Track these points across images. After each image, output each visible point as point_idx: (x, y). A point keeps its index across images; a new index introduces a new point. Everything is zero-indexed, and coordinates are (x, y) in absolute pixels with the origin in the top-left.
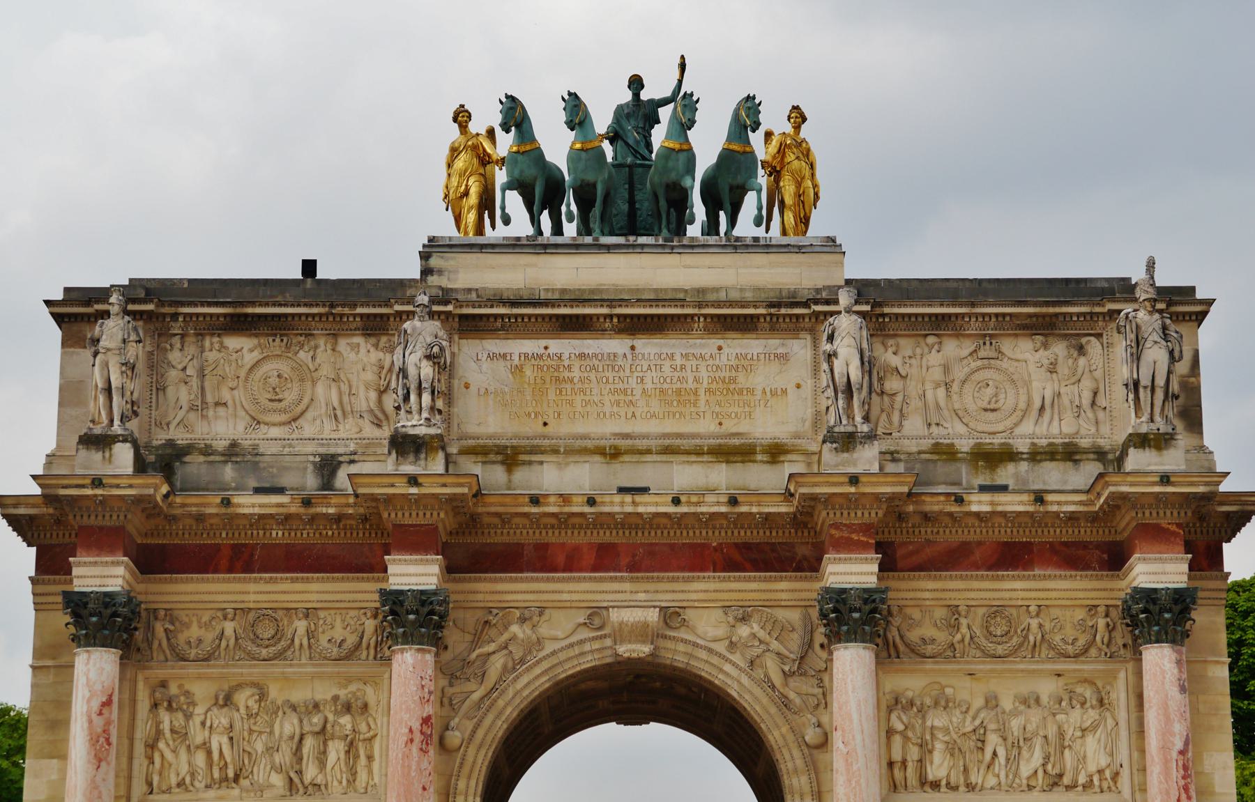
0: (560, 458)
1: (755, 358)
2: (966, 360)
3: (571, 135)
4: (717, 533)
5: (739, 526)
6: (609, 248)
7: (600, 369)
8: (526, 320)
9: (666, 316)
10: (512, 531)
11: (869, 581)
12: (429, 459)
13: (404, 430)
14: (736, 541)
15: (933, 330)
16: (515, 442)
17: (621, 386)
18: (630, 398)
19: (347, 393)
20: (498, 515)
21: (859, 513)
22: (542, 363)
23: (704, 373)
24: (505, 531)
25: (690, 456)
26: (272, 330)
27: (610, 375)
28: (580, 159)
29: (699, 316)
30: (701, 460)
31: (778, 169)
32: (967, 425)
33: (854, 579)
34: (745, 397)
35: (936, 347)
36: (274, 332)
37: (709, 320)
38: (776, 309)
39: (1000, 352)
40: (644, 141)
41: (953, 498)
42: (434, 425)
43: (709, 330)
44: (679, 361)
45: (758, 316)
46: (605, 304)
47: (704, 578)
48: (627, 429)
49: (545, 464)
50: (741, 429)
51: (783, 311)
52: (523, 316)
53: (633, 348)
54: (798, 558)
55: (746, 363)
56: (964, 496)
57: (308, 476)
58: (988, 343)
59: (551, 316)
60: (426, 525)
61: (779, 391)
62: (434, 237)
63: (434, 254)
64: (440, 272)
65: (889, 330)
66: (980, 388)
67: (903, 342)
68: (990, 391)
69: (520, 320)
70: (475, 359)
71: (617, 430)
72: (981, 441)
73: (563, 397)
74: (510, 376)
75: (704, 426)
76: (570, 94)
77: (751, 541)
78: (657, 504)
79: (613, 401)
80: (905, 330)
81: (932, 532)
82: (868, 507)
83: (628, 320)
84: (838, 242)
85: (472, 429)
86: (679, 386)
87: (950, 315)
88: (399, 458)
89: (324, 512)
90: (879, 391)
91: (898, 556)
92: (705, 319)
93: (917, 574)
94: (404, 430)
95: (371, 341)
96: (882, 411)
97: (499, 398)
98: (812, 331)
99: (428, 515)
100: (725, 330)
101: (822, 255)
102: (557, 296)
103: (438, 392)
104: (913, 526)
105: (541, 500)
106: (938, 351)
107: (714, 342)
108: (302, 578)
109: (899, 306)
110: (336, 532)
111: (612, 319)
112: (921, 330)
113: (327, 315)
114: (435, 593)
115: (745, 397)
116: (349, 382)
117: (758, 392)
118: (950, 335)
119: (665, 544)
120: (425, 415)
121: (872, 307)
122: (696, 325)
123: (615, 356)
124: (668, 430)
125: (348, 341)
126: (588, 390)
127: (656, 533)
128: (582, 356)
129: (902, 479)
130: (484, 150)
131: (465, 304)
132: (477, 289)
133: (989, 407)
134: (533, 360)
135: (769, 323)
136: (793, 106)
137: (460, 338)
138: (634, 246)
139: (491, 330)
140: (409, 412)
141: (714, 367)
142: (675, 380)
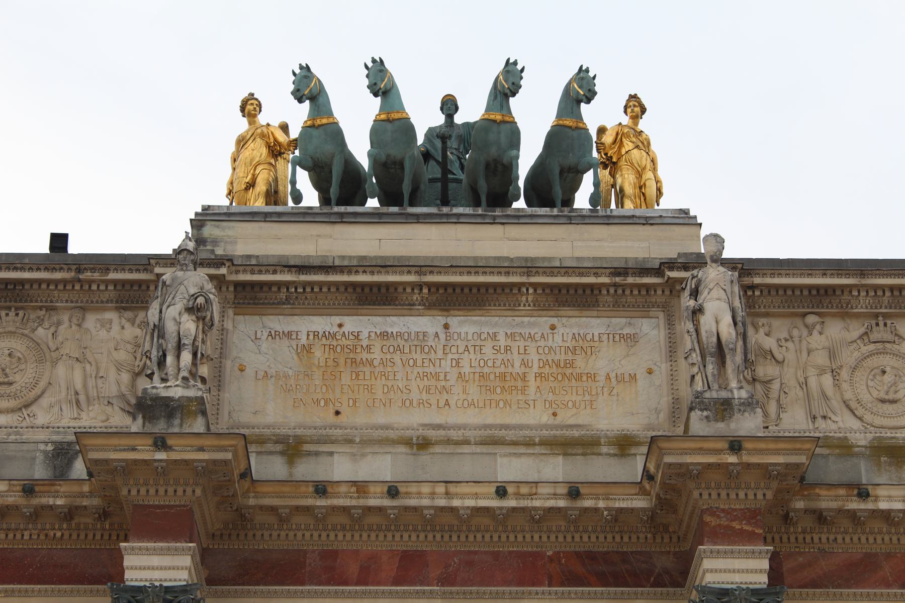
0: (354, 449)
1: (596, 338)
2: (855, 345)
3: (376, 102)
4: (553, 538)
5: (581, 529)
6: (418, 219)
7: (407, 350)
8: (316, 289)
9: (487, 286)
10: (291, 534)
11: (758, 581)
12: (184, 425)
13: (154, 391)
14: (577, 549)
15: (813, 307)
16: (299, 432)
17: (431, 369)
18: (443, 383)
19: (94, 376)
20: (273, 509)
21: (742, 495)
22: (335, 343)
23: (534, 357)
24: (283, 534)
25: (517, 447)
26: (5, 302)
27: (418, 356)
30: (532, 452)
31: (614, 160)
32: (860, 419)
33: (737, 578)
35: (818, 327)
36: (8, 304)
38: (622, 278)
39: (896, 335)
40: (458, 162)
41: (856, 492)
42: (194, 386)
43: (539, 306)
44: (502, 341)
46: (413, 269)
47: (537, 593)
48: (438, 420)
49: (336, 456)
50: (580, 422)
51: (630, 280)
52: (312, 284)
53: (446, 326)
54: (657, 571)
55: (586, 344)
56: (870, 488)
57: (37, 468)
58: (881, 323)
59: (347, 285)
60: (177, 506)
61: (627, 378)
62: (209, 206)
63: (208, 223)
64: (215, 242)
65: (759, 307)
66: (874, 376)
67: (776, 323)
69: (308, 289)
70: (253, 338)
71: (427, 421)
72: (881, 435)
73: (360, 382)
74: (295, 357)
76: (374, 61)
77: (596, 549)
78: (476, 496)
79: (421, 387)
80: (779, 307)
81: (828, 539)
82: (753, 485)
83: (441, 291)
84: (692, 214)
85: (245, 417)
86: (503, 369)
88: (147, 424)
89: (51, 503)
91: (784, 569)
92: (535, 290)
93: (811, 591)
94: (154, 391)
95: (126, 315)
97: (281, 383)
99: (180, 492)
100: (559, 306)
101: (674, 227)
102: (355, 263)
103: (202, 355)
104: (804, 532)
105: (329, 490)
107: (545, 321)
108: (20, 591)
109: (772, 275)
110: (67, 534)
111: (421, 289)
112: (799, 307)
113: (73, 281)
114: (184, 590)
115: (585, 384)
116: (97, 363)
117: (601, 378)
118: (834, 315)
119: (486, 553)
120: (185, 373)
122: (524, 298)
123: (424, 336)
124: (489, 421)
125: (99, 317)
126: (391, 374)
127: (475, 537)
128: (384, 335)
129: (798, 446)
130: (275, 140)
131: (241, 268)
132: (258, 256)
133: (887, 397)
134: (324, 339)
136: (630, 95)
137: (235, 314)
138: (447, 215)
139: (274, 304)
140: (164, 380)
141: (546, 350)
142: (498, 363)
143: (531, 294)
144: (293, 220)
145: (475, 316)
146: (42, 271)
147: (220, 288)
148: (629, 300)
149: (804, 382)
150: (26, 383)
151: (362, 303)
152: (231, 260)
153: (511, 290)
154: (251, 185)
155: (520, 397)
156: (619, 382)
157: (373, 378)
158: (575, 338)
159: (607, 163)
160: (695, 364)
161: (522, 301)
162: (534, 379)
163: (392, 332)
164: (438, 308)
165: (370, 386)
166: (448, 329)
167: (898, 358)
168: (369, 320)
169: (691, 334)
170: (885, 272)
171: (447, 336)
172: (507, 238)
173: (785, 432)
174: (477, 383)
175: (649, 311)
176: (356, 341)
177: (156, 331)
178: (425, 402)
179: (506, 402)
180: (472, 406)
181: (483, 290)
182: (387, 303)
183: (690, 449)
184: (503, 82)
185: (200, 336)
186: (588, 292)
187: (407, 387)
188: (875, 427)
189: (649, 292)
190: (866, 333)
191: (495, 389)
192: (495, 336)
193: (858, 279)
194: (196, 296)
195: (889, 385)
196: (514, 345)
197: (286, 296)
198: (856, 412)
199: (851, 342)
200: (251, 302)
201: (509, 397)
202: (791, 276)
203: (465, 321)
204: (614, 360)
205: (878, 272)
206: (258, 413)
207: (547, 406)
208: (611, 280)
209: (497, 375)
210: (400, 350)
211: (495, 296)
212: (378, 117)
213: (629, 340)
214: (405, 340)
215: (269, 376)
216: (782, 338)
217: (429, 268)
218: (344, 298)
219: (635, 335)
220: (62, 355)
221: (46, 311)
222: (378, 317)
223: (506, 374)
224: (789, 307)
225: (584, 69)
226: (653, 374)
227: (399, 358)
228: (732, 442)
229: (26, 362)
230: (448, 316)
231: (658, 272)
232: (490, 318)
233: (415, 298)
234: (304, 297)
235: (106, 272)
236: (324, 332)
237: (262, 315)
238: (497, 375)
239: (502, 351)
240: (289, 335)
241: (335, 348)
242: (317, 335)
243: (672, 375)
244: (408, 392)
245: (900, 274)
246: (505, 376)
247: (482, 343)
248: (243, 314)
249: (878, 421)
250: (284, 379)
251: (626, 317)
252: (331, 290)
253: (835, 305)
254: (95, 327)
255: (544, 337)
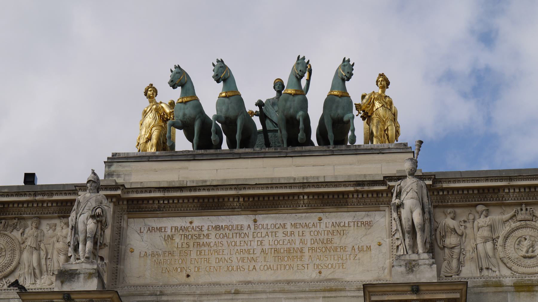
1: (347, 225)
2: (508, 223)
7: (231, 236)
15: (481, 201)
17: (245, 247)
18: (252, 256)
19: (44, 258)
27: (238, 240)
28: (224, 103)
29: (303, 194)
31: (369, 114)
32: (510, 269)
34: (339, 253)
35: (484, 213)
37: (311, 197)
39: (534, 216)
44: (289, 229)
45: (348, 193)
50: (336, 276)
51: (366, 188)
52: (173, 198)
53: (255, 221)
55: (341, 229)
58: (524, 209)
59: (194, 198)
61: (365, 249)
65: (448, 202)
66: (520, 242)
67: (458, 211)
68: (526, 243)
69: (171, 201)
70: (139, 232)
71: (242, 279)
73: (202, 257)
74: (164, 243)
75: (311, 274)
76: (218, 61)
79: (239, 259)
80: (460, 201)
83: (251, 200)
84: (409, 146)
86: (289, 246)
87: (494, 188)
90: (441, 246)
92: (308, 197)
95: (64, 221)
96: (445, 260)
98: (388, 203)
100: (324, 206)
106: (486, 217)
111: (239, 199)
112: (472, 201)
115: (339, 253)
117: (349, 249)
118: (495, 205)
121: (433, 183)
124: (280, 278)
128: (217, 228)
129: (454, 287)
130: (164, 111)
131: (130, 190)
133: (527, 255)
134: (181, 231)
135: (357, 198)
137: (128, 218)
139: (151, 211)
142: (286, 242)
143: (306, 199)
144: (132, 161)
145: (273, 214)
146: (14, 196)
147: (119, 203)
148: (366, 201)
149: (475, 247)
150: (5, 263)
151: (203, 208)
152: (123, 186)
153: (294, 197)
154: (149, 139)
155: (299, 263)
156: (360, 251)
157: (210, 254)
158: (334, 225)
159: (365, 116)
160: (399, 239)
161: (301, 204)
162: (308, 252)
163: (222, 226)
164: (250, 210)
165: (208, 259)
166: (256, 222)
167: (534, 230)
168: (208, 219)
169: (396, 220)
170: (525, 177)
171: (255, 227)
172: (294, 165)
173: (462, 279)
174: (273, 255)
175: (379, 207)
176: (200, 231)
177: (74, 230)
178: (241, 268)
179: (290, 266)
180: (270, 269)
181: (276, 198)
182: (219, 208)
183: (387, 291)
184: (296, 70)
185: (99, 232)
186: (341, 196)
187: (230, 259)
188: (519, 274)
189: (379, 196)
190: (514, 216)
191: (284, 257)
192: (285, 226)
193: (508, 182)
194: (96, 208)
195: (528, 247)
196: (296, 231)
197: (158, 206)
198: (507, 265)
199: (506, 221)
200: (138, 210)
201: (292, 263)
202: (261, 189)
203: (267, 217)
204: (357, 238)
205: (520, 177)
206: (140, 277)
207: (316, 267)
208: (354, 188)
209: (285, 249)
210: (227, 236)
211: (284, 201)
212: (221, 95)
213: (367, 225)
214: (230, 230)
215: (148, 255)
216: (462, 220)
217: (243, 186)
218: (193, 206)
219: (371, 222)
220: (26, 246)
221: (18, 219)
222: (213, 217)
223: (291, 249)
224: (466, 201)
225: (346, 59)
226: (381, 246)
227: (226, 241)
228: (412, 286)
229: (5, 251)
230: (256, 214)
231: (382, 182)
232: (281, 215)
233: (236, 204)
234: (169, 206)
235: (51, 196)
236: (181, 227)
237: (144, 218)
238: (285, 249)
239: (289, 235)
240: (160, 229)
241: (187, 237)
242: (177, 229)
243: (392, 246)
244: (231, 261)
245: (534, 178)
246: (290, 250)
247: (277, 230)
248: (134, 218)
249: (521, 270)
250: (156, 256)
251: (365, 211)
252: (185, 201)
253: (495, 199)
254: (46, 229)
255: (314, 225)
